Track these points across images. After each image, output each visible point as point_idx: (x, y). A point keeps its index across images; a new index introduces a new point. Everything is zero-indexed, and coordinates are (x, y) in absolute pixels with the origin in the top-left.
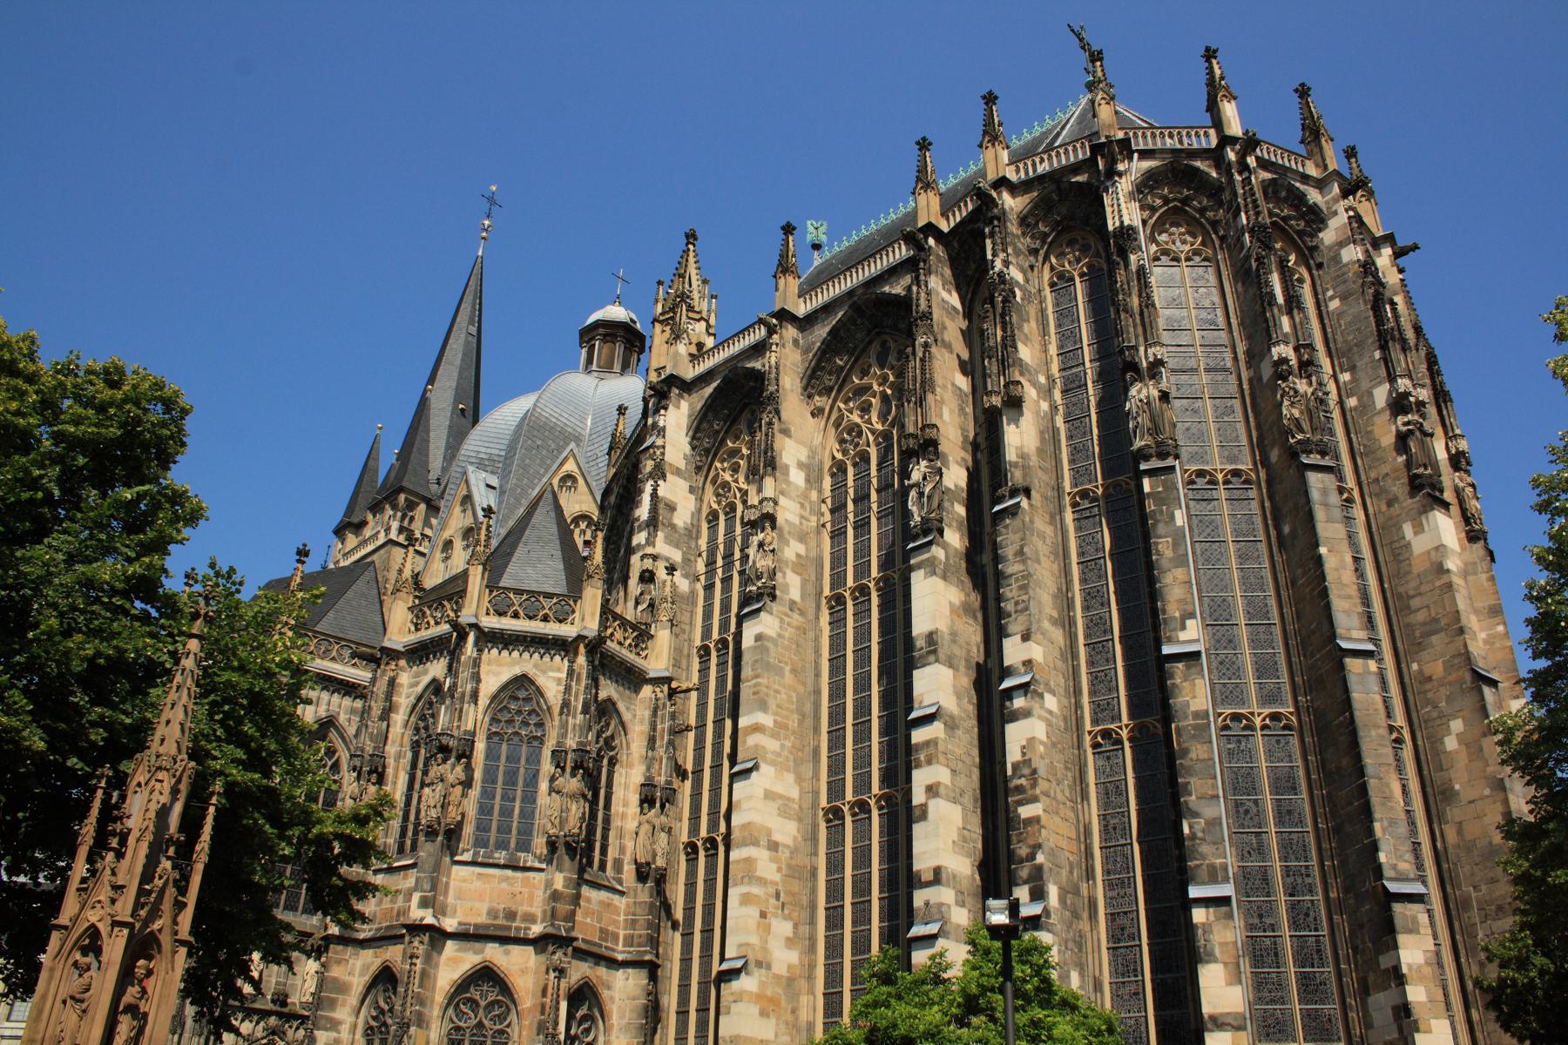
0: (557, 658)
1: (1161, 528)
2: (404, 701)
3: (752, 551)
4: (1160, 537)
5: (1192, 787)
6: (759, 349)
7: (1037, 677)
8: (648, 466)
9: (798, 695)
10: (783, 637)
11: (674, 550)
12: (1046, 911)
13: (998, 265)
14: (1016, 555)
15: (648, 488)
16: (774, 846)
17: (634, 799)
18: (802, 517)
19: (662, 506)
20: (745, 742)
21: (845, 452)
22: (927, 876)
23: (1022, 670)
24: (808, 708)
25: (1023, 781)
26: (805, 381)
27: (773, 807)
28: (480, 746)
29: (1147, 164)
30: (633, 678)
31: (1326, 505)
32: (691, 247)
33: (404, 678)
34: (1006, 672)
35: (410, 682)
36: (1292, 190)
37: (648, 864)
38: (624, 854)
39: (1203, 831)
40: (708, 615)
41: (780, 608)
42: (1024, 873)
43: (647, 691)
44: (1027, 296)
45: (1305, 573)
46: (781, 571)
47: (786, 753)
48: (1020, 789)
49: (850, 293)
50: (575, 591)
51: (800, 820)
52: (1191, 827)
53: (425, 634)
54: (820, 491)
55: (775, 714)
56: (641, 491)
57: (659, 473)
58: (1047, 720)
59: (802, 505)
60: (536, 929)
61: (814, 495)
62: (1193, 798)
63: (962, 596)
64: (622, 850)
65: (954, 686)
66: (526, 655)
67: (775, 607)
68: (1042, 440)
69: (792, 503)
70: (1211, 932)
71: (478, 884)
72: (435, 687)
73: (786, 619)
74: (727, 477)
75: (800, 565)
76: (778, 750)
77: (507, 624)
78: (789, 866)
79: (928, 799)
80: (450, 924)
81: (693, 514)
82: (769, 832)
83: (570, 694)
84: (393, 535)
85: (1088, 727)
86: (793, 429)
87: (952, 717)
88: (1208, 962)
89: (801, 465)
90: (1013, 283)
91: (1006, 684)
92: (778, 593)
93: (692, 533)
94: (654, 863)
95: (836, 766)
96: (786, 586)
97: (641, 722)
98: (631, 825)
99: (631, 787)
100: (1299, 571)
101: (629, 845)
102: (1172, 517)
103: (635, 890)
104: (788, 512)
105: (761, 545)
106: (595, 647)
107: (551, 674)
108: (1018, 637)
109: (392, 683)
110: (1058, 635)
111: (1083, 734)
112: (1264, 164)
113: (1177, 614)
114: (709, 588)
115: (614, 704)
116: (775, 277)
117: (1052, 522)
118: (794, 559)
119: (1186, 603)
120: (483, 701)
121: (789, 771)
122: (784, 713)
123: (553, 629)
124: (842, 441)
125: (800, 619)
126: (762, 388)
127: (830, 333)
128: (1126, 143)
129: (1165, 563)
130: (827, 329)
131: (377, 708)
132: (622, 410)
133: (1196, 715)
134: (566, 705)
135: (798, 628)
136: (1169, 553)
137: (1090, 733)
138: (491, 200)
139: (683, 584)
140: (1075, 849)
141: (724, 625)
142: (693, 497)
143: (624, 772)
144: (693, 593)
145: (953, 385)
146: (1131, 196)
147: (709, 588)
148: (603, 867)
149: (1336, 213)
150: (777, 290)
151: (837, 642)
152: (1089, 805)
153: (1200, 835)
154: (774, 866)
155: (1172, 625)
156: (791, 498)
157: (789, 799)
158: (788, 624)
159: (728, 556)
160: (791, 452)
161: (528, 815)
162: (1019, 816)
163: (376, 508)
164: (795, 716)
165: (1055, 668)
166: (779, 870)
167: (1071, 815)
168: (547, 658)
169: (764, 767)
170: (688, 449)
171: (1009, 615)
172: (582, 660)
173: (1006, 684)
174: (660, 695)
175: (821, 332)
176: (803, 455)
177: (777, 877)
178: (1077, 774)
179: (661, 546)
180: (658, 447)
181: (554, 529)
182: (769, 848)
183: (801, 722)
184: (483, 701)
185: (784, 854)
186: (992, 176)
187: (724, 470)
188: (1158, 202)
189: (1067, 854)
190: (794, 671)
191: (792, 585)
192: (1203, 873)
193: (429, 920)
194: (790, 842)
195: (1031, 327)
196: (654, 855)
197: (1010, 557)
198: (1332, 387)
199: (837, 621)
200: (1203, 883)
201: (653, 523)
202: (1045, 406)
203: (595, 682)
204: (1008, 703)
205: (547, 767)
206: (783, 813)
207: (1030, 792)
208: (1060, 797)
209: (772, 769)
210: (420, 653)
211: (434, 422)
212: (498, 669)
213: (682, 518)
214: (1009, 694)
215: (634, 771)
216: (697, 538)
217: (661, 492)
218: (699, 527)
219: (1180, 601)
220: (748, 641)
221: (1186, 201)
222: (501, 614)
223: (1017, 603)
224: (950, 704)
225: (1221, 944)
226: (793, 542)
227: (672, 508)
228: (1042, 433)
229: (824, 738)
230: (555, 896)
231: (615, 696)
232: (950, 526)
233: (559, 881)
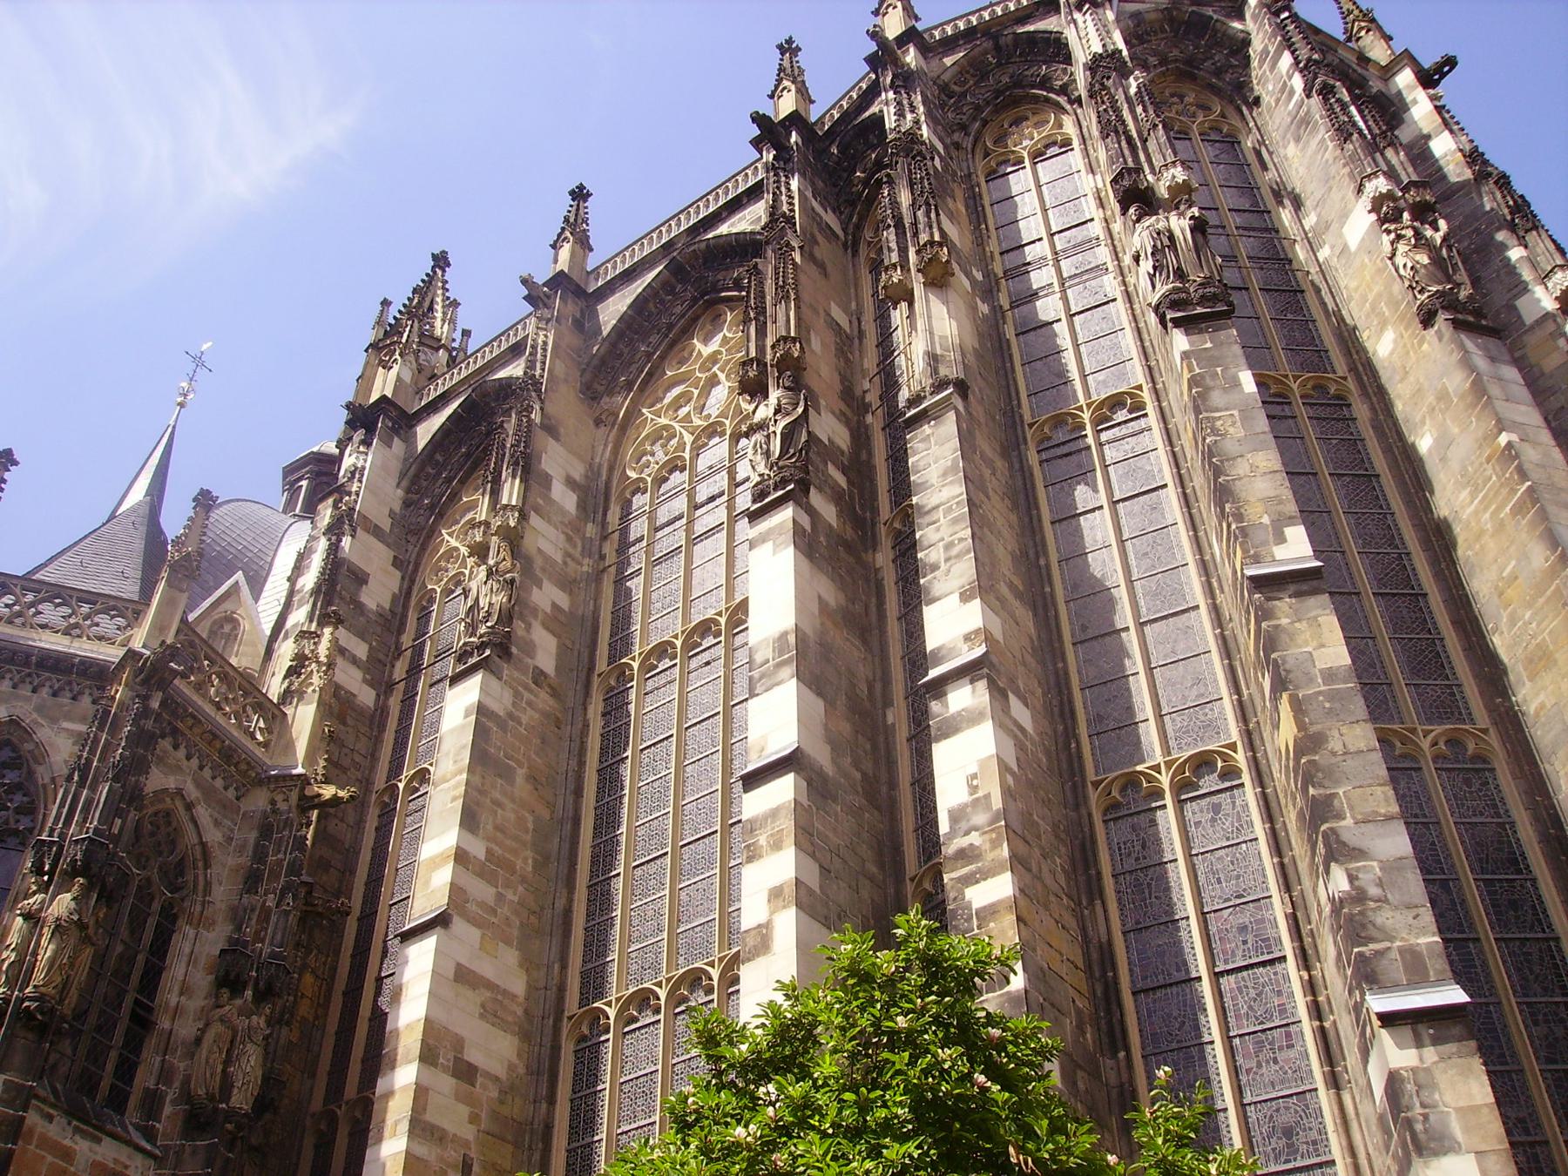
0: (86, 700)
1: (1217, 398)
4: (1217, 410)
5: (1341, 802)
7: (994, 659)
9: (537, 820)
10: (520, 723)
11: (355, 639)
14: (945, 474)
16: (465, 1072)
17: (202, 981)
18: (567, 555)
19: (344, 570)
20: (427, 882)
23: (965, 647)
25: (975, 838)
26: (588, 375)
27: (472, 999)
32: (439, 272)
34: (937, 658)
37: (211, 1098)
38: (169, 1083)
39: (1380, 884)
41: (516, 674)
43: (258, 801)
45: (1473, 496)
46: (522, 618)
47: (504, 911)
48: (965, 855)
51: (525, 1036)
52: (1352, 878)
54: (604, 524)
55: (488, 839)
58: (1015, 737)
59: (569, 539)
61: (591, 530)
62: (1349, 821)
63: (843, 602)
64: (166, 1075)
65: (826, 728)
66: (26, 691)
67: (507, 670)
69: (552, 529)
70: (1434, 1086)
73: (526, 695)
75: (556, 621)
76: (491, 901)
78: (495, 1116)
79: (772, 913)
81: (394, 595)
82: (459, 1044)
83: (92, 752)
85: (1091, 776)
86: (562, 430)
87: (821, 773)
88: (1436, 1153)
89: (570, 483)
92: (514, 650)
94: (227, 1099)
96: (529, 649)
97: (241, 849)
98: (186, 1029)
99: (203, 961)
100: (1465, 494)
102: (1236, 384)
103: (179, 1153)
107: (65, 725)
108: (956, 595)
111: (1084, 786)
113: (1266, 520)
115: (189, 807)
116: (554, 246)
118: (548, 610)
119: (1281, 502)
121: (508, 943)
122: (508, 842)
125: (551, 702)
127: (630, 307)
129: (1230, 446)
130: (629, 301)
133: (1330, 675)
135: (545, 714)
136: (1237, 432)
137: (1096, 784)
138: (199, 360)
139: (366, 696)
140: (1084, 988)
142: (398, 574)
143: (191, 932)
144: (382, 711)
145: (829, 315)
148: (118, 1101)
149: (1415, 102)
150: (556, 261)
152: (1103, 903)
153: (1374, 891)
154: (464, 1111)
155: (1257, 536)
156: (549, 522)
157: (505, 992)
158: (530, 704)
162: (969, 906)
164: (529, 853)
165: (1024, 664)
166: (474, 1119)
167: (1072, 923)
168: (65, 700)
169: (458, 924)
170: (397, 507)
171: (935, 567)
174: (282, 806)
176: (578, 471)
177: (468, 1132)
178: (1078, 855)
180: (349, 494)
181: (139, 545)
182: (454, 1075)
185: (487, 1093)
187: (450, 535)
188: (1153, 60)
189: (1071, 990)
190: (532, 778)
192: (1393, 967)
194: (499, 1070)
196: (227, 1086)
197: (934, 481)
200: (1395, 987)
204: (935, 706)
206: (492, 1013)
207: (990, 856)
208: (1049, 880)
209: (475, 933)
213: (378, 594)
214: (939, 687)
215: (211, 936)
216: (401, 629)
218: (404, 616)
219: (1267, 500)
223: (949, 546)
224: (821, 755)
225: (1458, 1110)
226: (547, 585)
227: (360, 578)
231: (192, 792)
232: (820, 489)
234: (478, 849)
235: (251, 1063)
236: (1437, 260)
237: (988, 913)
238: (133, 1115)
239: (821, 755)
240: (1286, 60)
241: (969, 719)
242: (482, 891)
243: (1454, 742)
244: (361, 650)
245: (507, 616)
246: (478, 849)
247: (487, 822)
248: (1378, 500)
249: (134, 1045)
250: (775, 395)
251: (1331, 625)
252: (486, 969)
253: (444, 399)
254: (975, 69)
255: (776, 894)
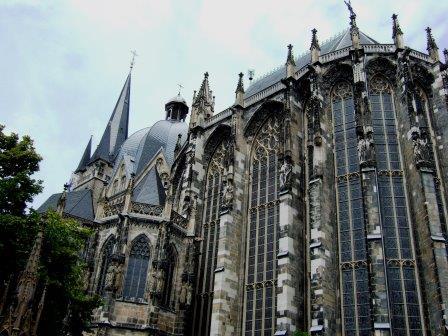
2: (101, 242)
3: (224, 192)
6: (229, 118)
8: (189, 159)
12: (323, 329)
13: (315, 94)
15: (189, 166)
16: (228, 299)
21: (258, 157)
22: (282, 313)
24: (242, 249)
27: (229, 284)
28: (127, 259)
29: (370, 58)
30: (184, 236)
31: (429, 186)
33: (101, 234)
34: (312, 241)
35: (105, 235)
36: (422, 67)
40: (208, 213)
42: (316, 315)
43: (186, 241)
44: (324, 105)
48: (315, 284)
49: (262, 100)
50: (162, 203)
53: (109, 218)
56: (186, 168)
57: (193, 161)
60: (144, 326)
61: (247, 172)
64: (175, 298)
68: (328, 158)
71: (124, 309)
72: (112, 237)
74: (216, 163)
75: (241, 198)
77: (138, 215)
80: (114, 323)
84: (96, 175)
89: (243, 162)
90: (320, 101)
91: (313, 245)
93: (203, 183)
95: (251, 270)
98: (178, 289)
101: (177, 296)
104: (238, 178)
105: (228, 190)
106: (169, 225)
109: (97, 236)
110: (331, 228)
112: (412, 58)
114: (209, 203)
117: (330, 188)
120: (129, 243)
123: (154, 218)
124: (257, 153)
126: (230, 133)
128: (362, 50)
129: (369, 205)
131: (91, 244)
132: (180, 136)
133: (379, 261)
134: (158, 245)
139: (200, 201)
141: (214, 217)
146: (364, 70)
147: (209, 203)
151: (253, 226)
159: (216, 192)
160: (239, 157)
161: (142, 286)
163: (89, 165)
172: (163, 229)
173: (313, 245)
175: (251, 114)
179: (193, 189)
183: (240, 253)
184: (129, 243)
185: (232, 302)
186: (314, 61)
191: (238, 205)
193: (107, 322)
195: (325, 116)
198: (434, 142)
199: (254, 218)
201: (190, 179)
202: (329, 145)
203: (168, 238)
205: (150, 266)
206: (232, 287)
210: (108, 224)
211: (112, 134)
212: (135, 232)
213: (200, 178)
217: (193, 168)
220: (222, 224)
221: (383, 72)
222: (136, 212)
224: (292, 252)
227: (197, 174)
228: (328, 156)
229: (247, 260)
230: (152, 314)
233: (152, 309)
234: (228, 253)
235: (189, 295)
236: (423, 152)
237: (318, 296)
238: (171, 306)
239: (292, 252)
240: (403, 80)
241: (318, 257)
242: (229, 262)
243: (408, 263)
244: (198, 191)
245: (231, 201)
246: (228, 253)
247: (230, 248)
248: (403, 203)
249: (170, 291)
250: (286, 164)
251: (380, 249)
252: (231, 278)
253: (212, 126)
254: (331, 72)
255: (284, 281)
